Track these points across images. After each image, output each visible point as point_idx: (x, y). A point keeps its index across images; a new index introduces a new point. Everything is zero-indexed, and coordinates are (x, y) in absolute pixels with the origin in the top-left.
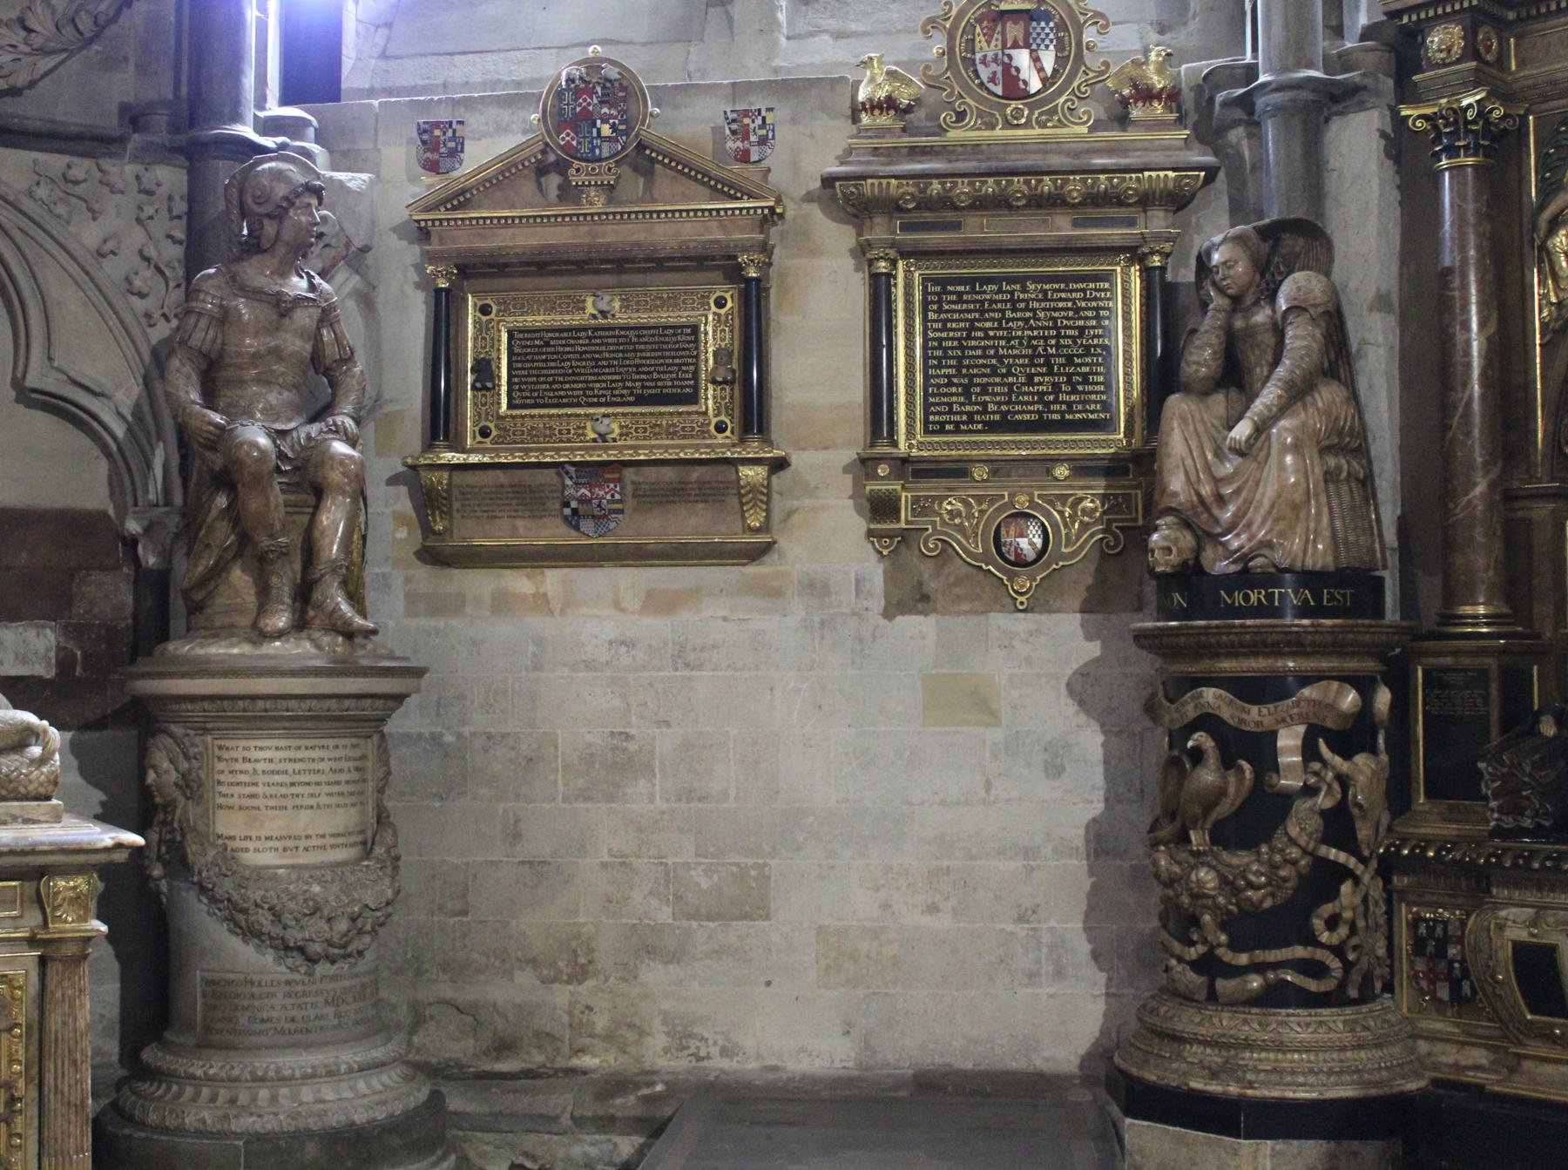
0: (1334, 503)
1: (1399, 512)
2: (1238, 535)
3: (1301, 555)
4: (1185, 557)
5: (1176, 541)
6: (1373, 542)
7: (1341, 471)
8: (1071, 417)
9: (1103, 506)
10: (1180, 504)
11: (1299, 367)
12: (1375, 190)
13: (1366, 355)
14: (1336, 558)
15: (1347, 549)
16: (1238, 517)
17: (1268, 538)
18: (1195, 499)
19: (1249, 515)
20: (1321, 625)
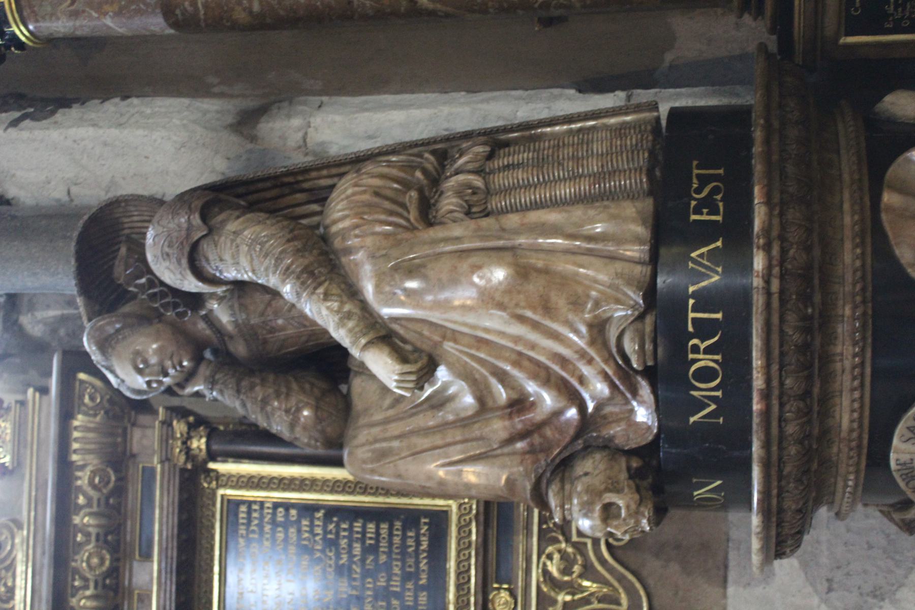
0: (525, 197)
1: (572, 92)
2: (582, 380)
3: (619, 266)
4: (623, 476)
5: (594, 493)
6: (606, 127)
7: (470, 186)
8: (424, 576)
9: (557, 541)
10: (527, 474)
11: (278, 260)
12: (85, 132)
13: (322, 143)
14: (630, 196)
15: (613, 173)
16: (547, 378)
17: (583, 329)
18: (519, 445)
19: (542, 359)
20: (767, 231)
